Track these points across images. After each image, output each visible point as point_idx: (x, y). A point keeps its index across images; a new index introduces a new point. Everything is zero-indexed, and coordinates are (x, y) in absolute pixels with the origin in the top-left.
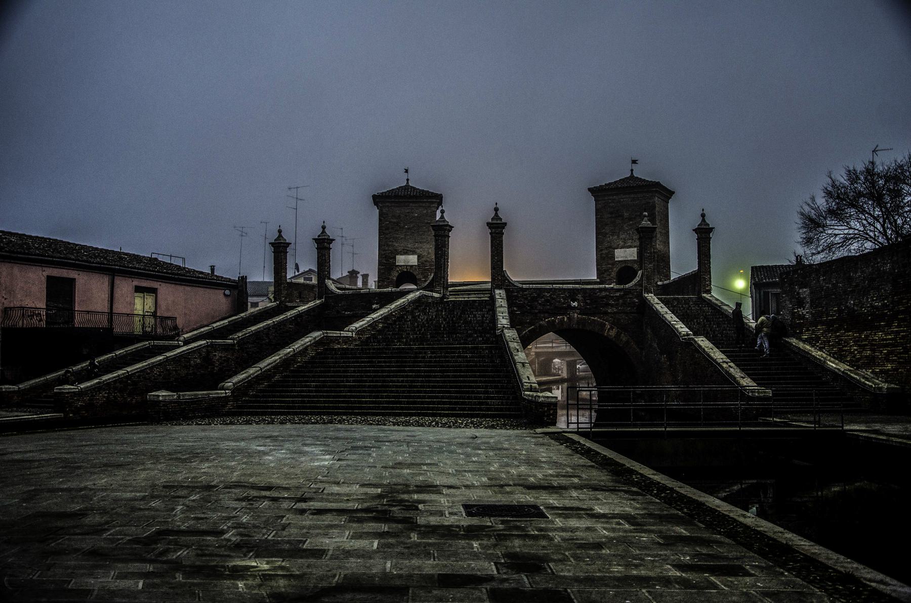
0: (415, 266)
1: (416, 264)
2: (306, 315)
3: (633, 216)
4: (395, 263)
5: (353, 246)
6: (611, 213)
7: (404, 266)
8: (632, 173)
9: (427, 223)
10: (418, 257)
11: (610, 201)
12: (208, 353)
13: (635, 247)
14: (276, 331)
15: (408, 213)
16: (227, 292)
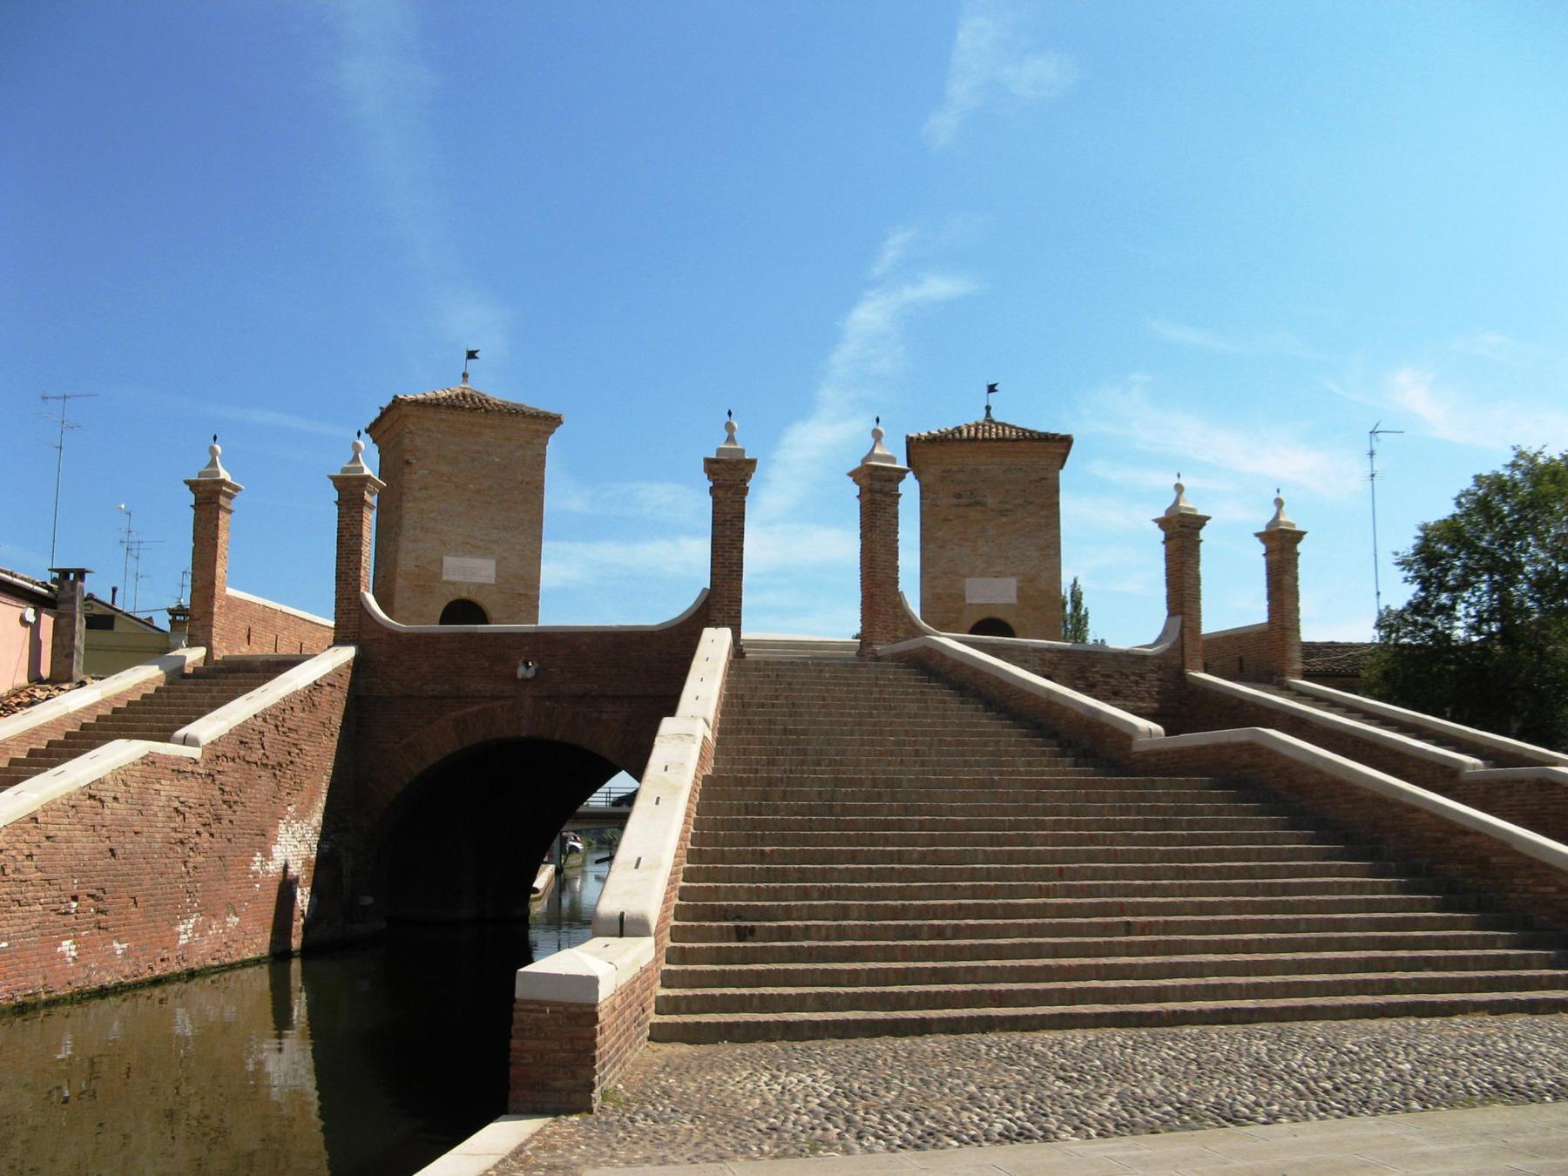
0: (491, 585)
1: (493, 581)
2: (329, 684)
3: (1009, 507)
4: (441, 573)
5: (137, 558)
6: (958, 496)
7: (462, 583)
8: (988, 414)
9: (528, 483)
10: (497, 563)
11: (955, 468)
12: (145, 780)
13: (1012, 575)
14: (276, 726)
15: (477, 452)
16: (30, 615)
